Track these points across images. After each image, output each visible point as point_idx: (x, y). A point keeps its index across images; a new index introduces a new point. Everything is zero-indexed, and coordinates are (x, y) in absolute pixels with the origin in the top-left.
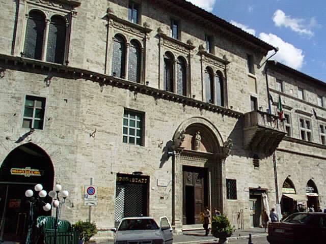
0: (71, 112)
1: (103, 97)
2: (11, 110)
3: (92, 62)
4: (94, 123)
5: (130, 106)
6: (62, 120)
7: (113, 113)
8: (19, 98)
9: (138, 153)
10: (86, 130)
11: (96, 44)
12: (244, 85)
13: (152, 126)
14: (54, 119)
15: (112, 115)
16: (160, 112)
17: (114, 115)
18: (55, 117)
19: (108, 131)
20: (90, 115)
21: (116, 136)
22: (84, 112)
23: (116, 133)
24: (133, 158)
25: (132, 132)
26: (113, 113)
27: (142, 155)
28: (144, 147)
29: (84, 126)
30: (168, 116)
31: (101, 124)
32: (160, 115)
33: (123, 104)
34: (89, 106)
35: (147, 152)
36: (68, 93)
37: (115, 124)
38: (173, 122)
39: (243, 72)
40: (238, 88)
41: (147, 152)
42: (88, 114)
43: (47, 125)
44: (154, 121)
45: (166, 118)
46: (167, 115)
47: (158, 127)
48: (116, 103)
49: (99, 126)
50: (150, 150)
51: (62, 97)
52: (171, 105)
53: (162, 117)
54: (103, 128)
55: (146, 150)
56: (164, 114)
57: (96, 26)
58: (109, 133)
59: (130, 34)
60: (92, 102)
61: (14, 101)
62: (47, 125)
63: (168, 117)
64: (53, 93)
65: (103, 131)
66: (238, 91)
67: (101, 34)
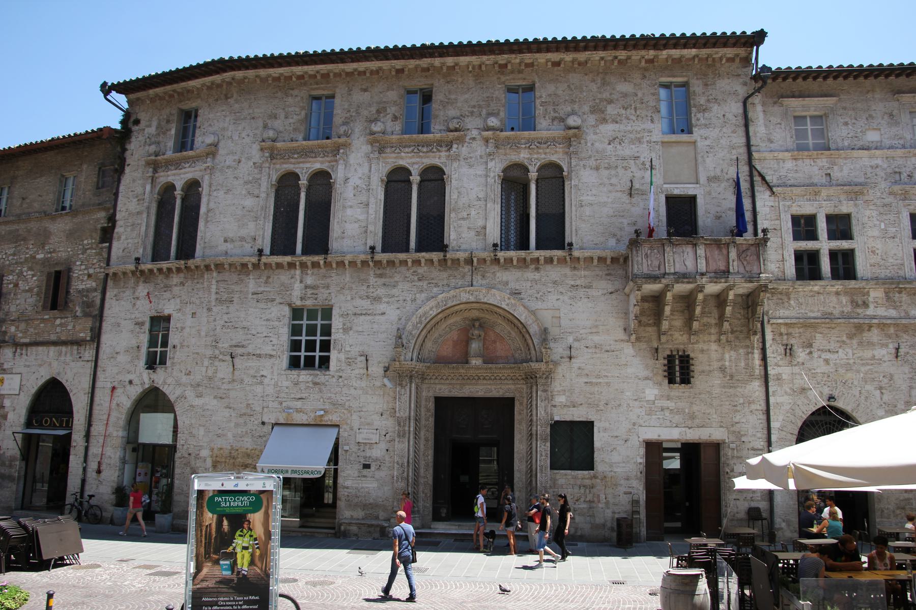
0: (199, 331)
1: (250, 296)
2: (134, 343)
3: (232, 241)
4: (234, 343)
5: (302, 299)
6: (188, 347)
7: (268, 320)
8: (142, 324)
9: (316, 384)
10: (221, 357)
11: (241, 207)
12: (638, 174)
13: (346, 330)
14: (178, 347)
15: (265, 323)
16: (368, 297)
17: (272, 323)
18: (181, 343)
19: (258, 352)
20: (229, 330)
21: (273, 360)
22: (218, 328)
23: (274, 353)
24: (303, 396)
25: (311, 346)
26: (268, 320)
27: (323, 387)
28: (327, 373)
29: (217, 352)
30: (388, 303)
31: (244, 343)
32: (366, 304)
33: (288, 299)
34: (225, 317)
35: (334, 380)
36: (198, 302)
37: (271, 339)
38: (398, 312)
39: (639, 140)
40: (618, 188)
41: (334, 380)
42: (225, 330)
43: (172, 356)
44: (353, 317)
45: (382, 307)
46: (385, 300)
47: (360, 329)
48: (273, 300)
49: (243, 346)
50: (341, 377)
51: (189, 310)
52: (396, 279)
53: (371, 307)
54: (250, 349)
55: (333, 377)
56: (377, 299)
57: (241, 175)
58: (259, 356)
59: (301, 165)
60: (232, 308)
61: (137, 329)
62: (172, 356)
63: (385, 305)
64: (178, 307)
65: (249, 354)
66: (619, 194)
67: (249, 186)
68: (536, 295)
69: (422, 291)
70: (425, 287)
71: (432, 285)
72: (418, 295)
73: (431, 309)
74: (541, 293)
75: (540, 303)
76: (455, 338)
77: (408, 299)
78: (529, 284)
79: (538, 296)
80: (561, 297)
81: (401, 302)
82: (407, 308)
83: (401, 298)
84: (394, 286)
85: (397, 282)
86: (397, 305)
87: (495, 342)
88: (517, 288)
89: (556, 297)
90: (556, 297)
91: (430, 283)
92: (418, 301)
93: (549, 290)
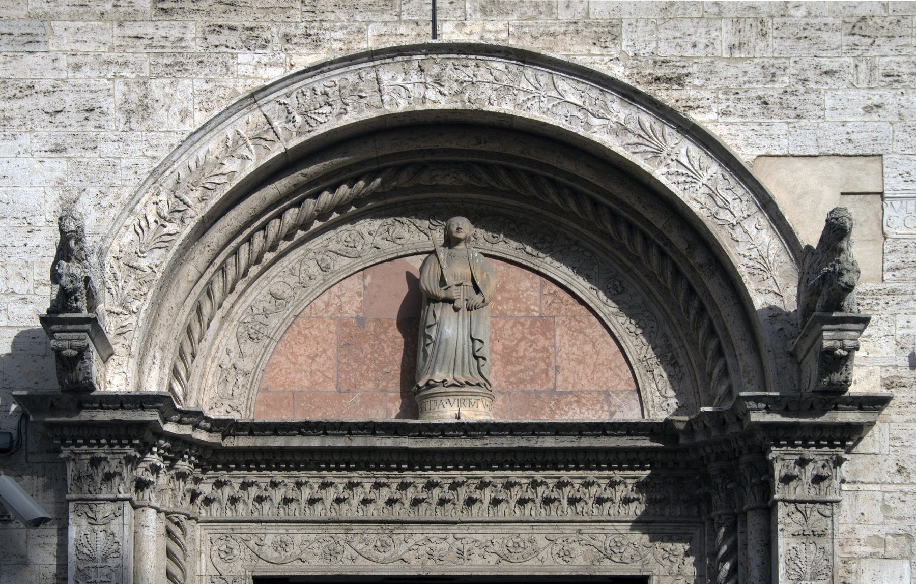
38: (59, 167)
68: (759, 89)
69: (181, 67)
70: (195, 47)
71: (226, 37)
72: (157, 89)
73: (230, 150)
74: (785, 81)
75: (779, 127)
76: (350, 311)
77: (109, 105)
78: (725, 36)
79: (773, 91)
80: (888, 96)
81: (73, 118)
82: (107, 149)
83: (69, 100)
84: (31, 40)
85: (45, 18)
86: (47, 134)
87: (545, 325)
88: (666, 51)
89: (860, 97)
90: (860, 97)
91: (218, 29)
92: (160, 114)
93: (827, 63)
